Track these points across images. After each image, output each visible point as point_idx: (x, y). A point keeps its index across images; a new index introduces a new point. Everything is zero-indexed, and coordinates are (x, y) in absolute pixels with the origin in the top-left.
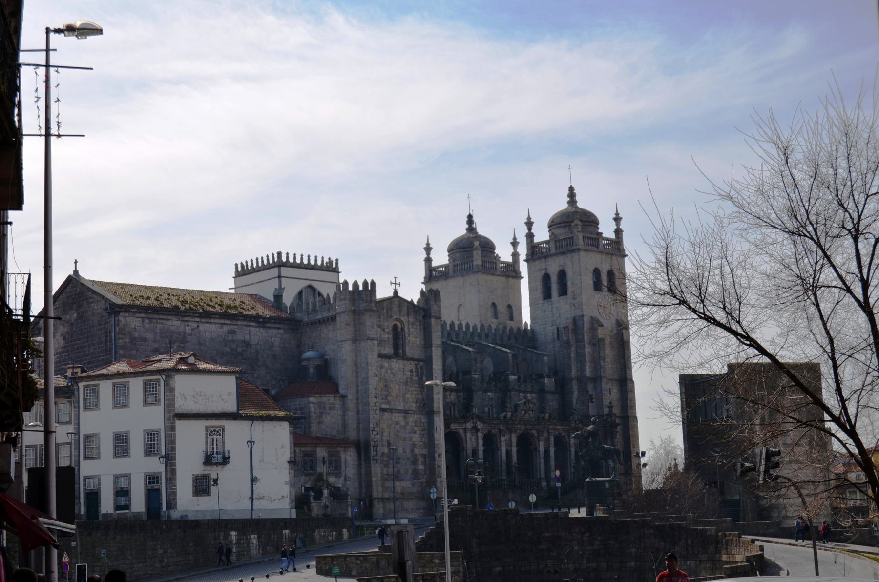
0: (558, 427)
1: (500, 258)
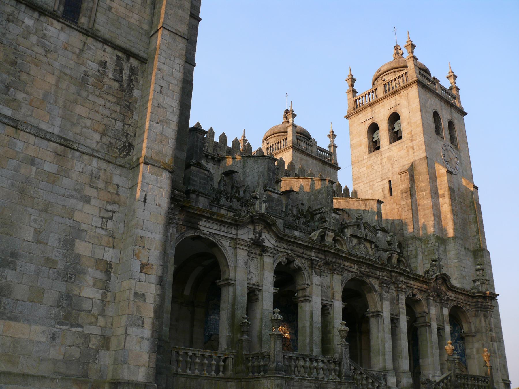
0: (412, 282)
1: (316, 143)
